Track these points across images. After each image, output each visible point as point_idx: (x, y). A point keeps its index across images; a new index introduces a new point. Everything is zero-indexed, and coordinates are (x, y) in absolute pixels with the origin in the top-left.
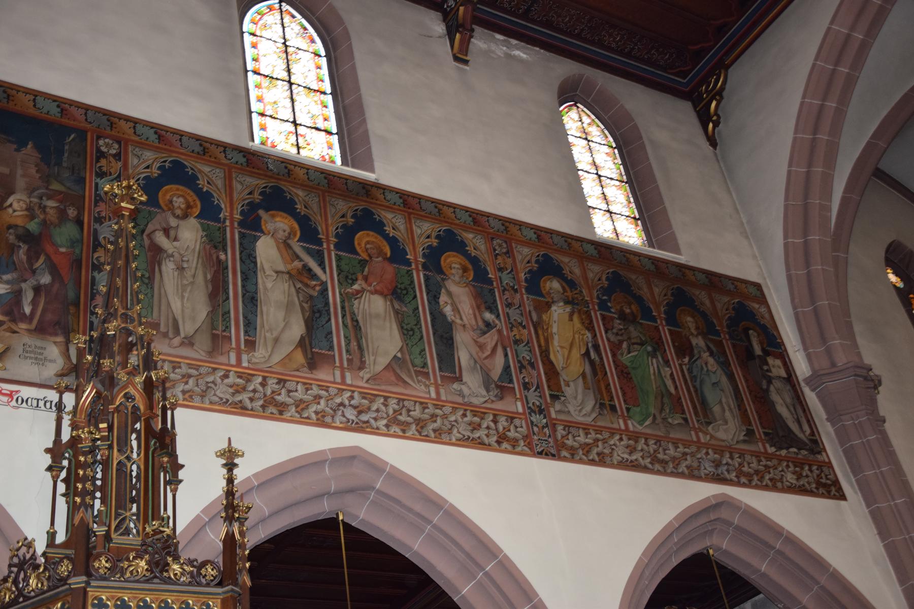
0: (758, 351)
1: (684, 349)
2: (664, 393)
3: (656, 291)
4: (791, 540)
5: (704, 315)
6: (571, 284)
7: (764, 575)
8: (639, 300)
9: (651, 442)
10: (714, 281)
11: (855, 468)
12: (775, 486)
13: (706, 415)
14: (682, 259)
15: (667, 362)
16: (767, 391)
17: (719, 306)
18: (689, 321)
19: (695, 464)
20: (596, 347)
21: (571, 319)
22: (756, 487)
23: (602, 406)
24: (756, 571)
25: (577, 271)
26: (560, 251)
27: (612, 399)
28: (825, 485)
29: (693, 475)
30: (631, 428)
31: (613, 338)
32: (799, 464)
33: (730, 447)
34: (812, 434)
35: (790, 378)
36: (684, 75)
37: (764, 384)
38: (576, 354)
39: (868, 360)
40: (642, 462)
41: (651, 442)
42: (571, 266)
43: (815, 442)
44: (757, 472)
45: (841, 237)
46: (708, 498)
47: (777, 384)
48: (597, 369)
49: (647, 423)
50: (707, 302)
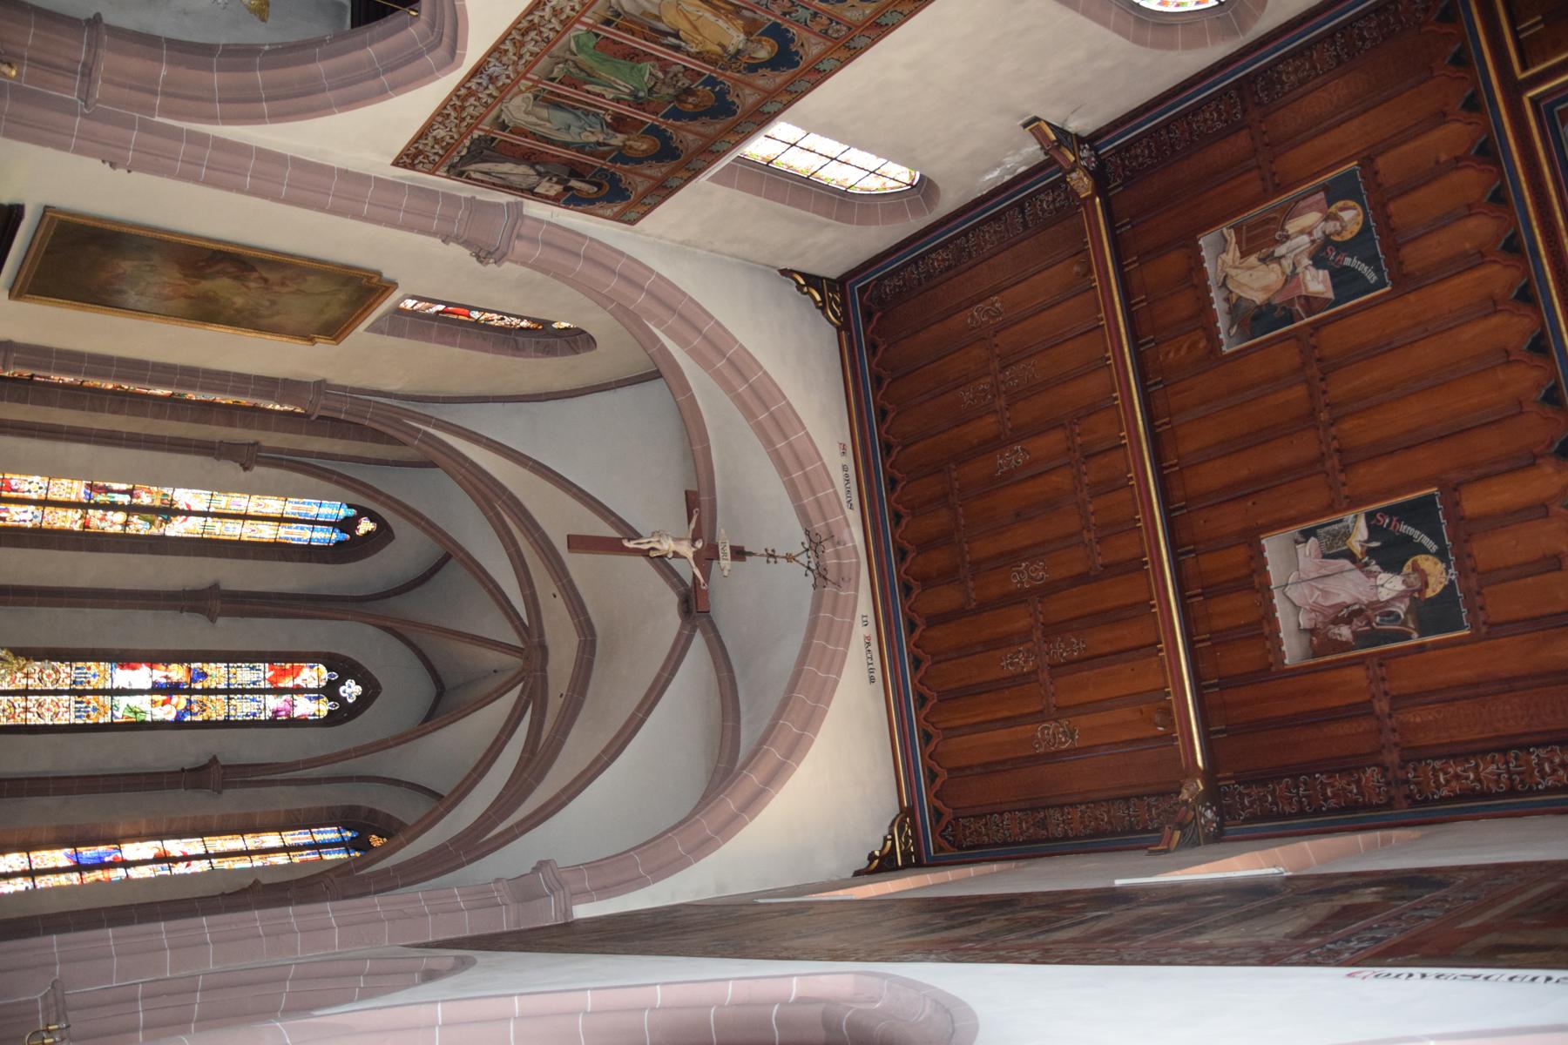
0: (574, 183)
1: (619, 123)
2: (591, 77)
3: (691, 137)
4: (381, 94)
5: (639, 161)
6: (753, 68)
7: (363, 46)
8: (693, 117)
9: (552, 35)
10: (663, 190)
11: (417, 191)
12: (441, 114)
13: (545, 100)
14: (703, 179)
15: (618, 101)
16: (532, 166)
17: (638, 179)
18: (642, 145)
19: (505, 59)
20: (677, 48)
21: (720, 45)
22: (449, 99)
23: (618, 15)
24: (372, 42)
25: (761, 82)
26: (791, 81)
27: (617, 28)
28: (416, 156)
29: (496, 50)
30: (577, 26)
31: (675, 68)
32: (448, 148)
33: (501, 100)
34: (468, 177)
35: (531, 192)
36: (862, 291)
37: (542, 169)
38: (683, 25)
39: (507, 265)
40: (538, 13)
41: (552, 35)
42: (768, 80)
43: (460, 174)
44: (463, 108)
45: (629, 318)
46: (465, 48)
47: (534, 179)
48: (657, 35)
49: (573, 44)
50: (648, 172)
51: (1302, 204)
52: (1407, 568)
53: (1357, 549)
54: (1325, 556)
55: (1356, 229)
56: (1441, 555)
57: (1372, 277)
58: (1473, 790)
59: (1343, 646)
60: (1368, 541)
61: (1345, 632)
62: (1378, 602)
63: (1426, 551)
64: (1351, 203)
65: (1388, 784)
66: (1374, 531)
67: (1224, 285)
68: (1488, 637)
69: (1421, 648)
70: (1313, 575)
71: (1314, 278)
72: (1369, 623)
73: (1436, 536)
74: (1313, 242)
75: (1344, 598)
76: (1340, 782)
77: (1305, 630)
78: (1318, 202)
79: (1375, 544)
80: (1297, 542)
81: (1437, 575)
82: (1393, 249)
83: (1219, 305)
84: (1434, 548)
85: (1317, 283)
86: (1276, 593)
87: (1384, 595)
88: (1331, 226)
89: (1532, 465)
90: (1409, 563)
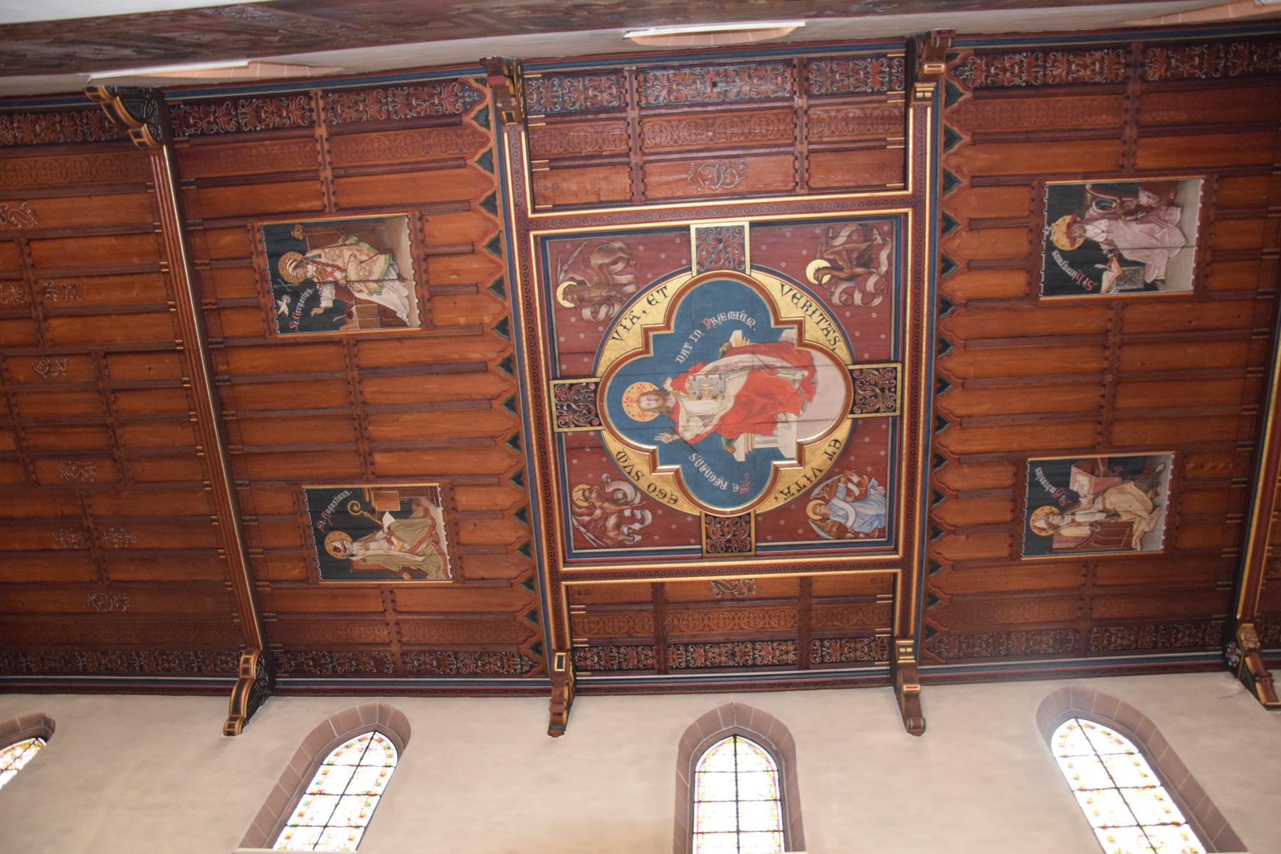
51: (1072, 545)
52: (1080, 242)
53: (1115, 266)
54: (1143, 265)
55: (1038, 511)
56: (1051, 247)
57: (1039, 472)
58: (1075, 55)
59: (1148, 187)
60: (1103, 270)
61: (1144, 199)
62: (1109, 219)
63: (1062, 252)
64: (1036, 531)
65: (1143, 65)
66: (1097, 278)
67: (1155, 507)
68: (1032, 177)
69: (1087, 176)
70: (1157, 251)
71: (1082, 486)
72: (1123, 203)
73: (1051, 263)
74: (1073, 514)
75: (1137, 228)
76: (1184, 69)
77: (1177, 206)
78: (1060, 542)
79: (1099, 266)
80: (1163, 282)
81: (1058, 233)
82: (1017, 487)
83: (1165, 492)
84: (1056, 255)
85: (1081, 482)
86: (1194, 241)
87: (1103, 224)
88: (1056, 520)
89: (969, 301)
90: (1077, 246)
